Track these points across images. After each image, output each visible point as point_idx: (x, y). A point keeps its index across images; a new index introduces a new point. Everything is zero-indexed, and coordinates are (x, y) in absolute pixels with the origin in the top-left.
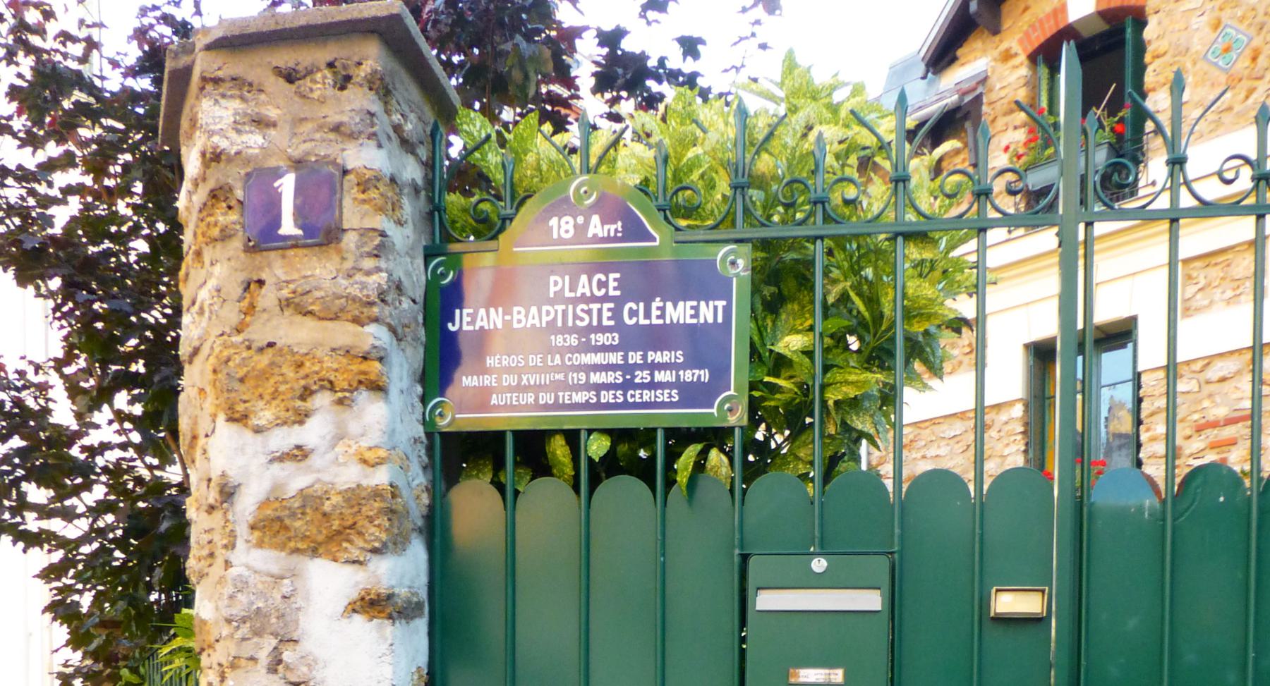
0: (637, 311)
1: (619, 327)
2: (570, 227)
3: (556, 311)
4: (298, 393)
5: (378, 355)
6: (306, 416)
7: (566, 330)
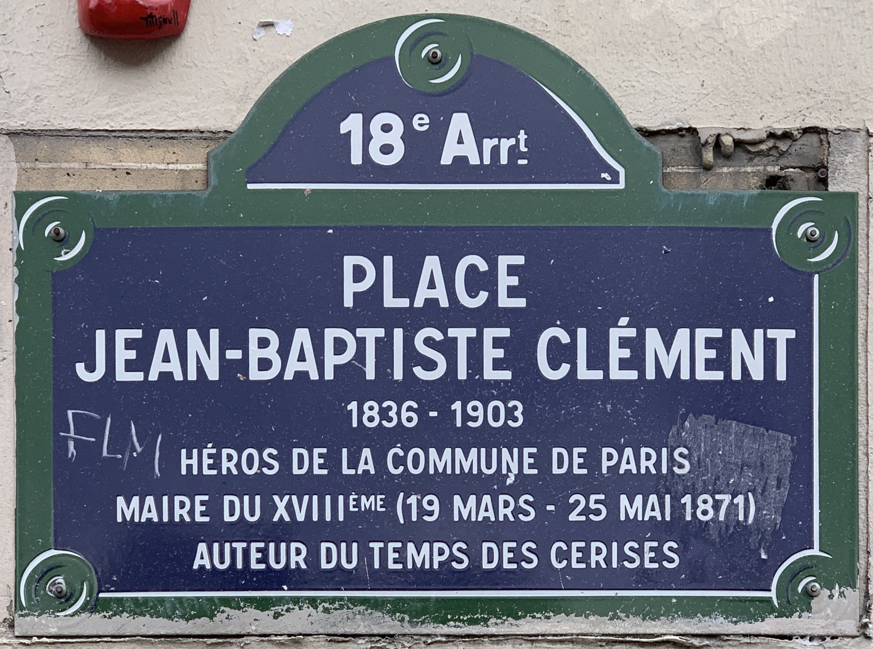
0: (573, 344)
2: (395, 138)
3: (361, 342)
7: (384, 388)
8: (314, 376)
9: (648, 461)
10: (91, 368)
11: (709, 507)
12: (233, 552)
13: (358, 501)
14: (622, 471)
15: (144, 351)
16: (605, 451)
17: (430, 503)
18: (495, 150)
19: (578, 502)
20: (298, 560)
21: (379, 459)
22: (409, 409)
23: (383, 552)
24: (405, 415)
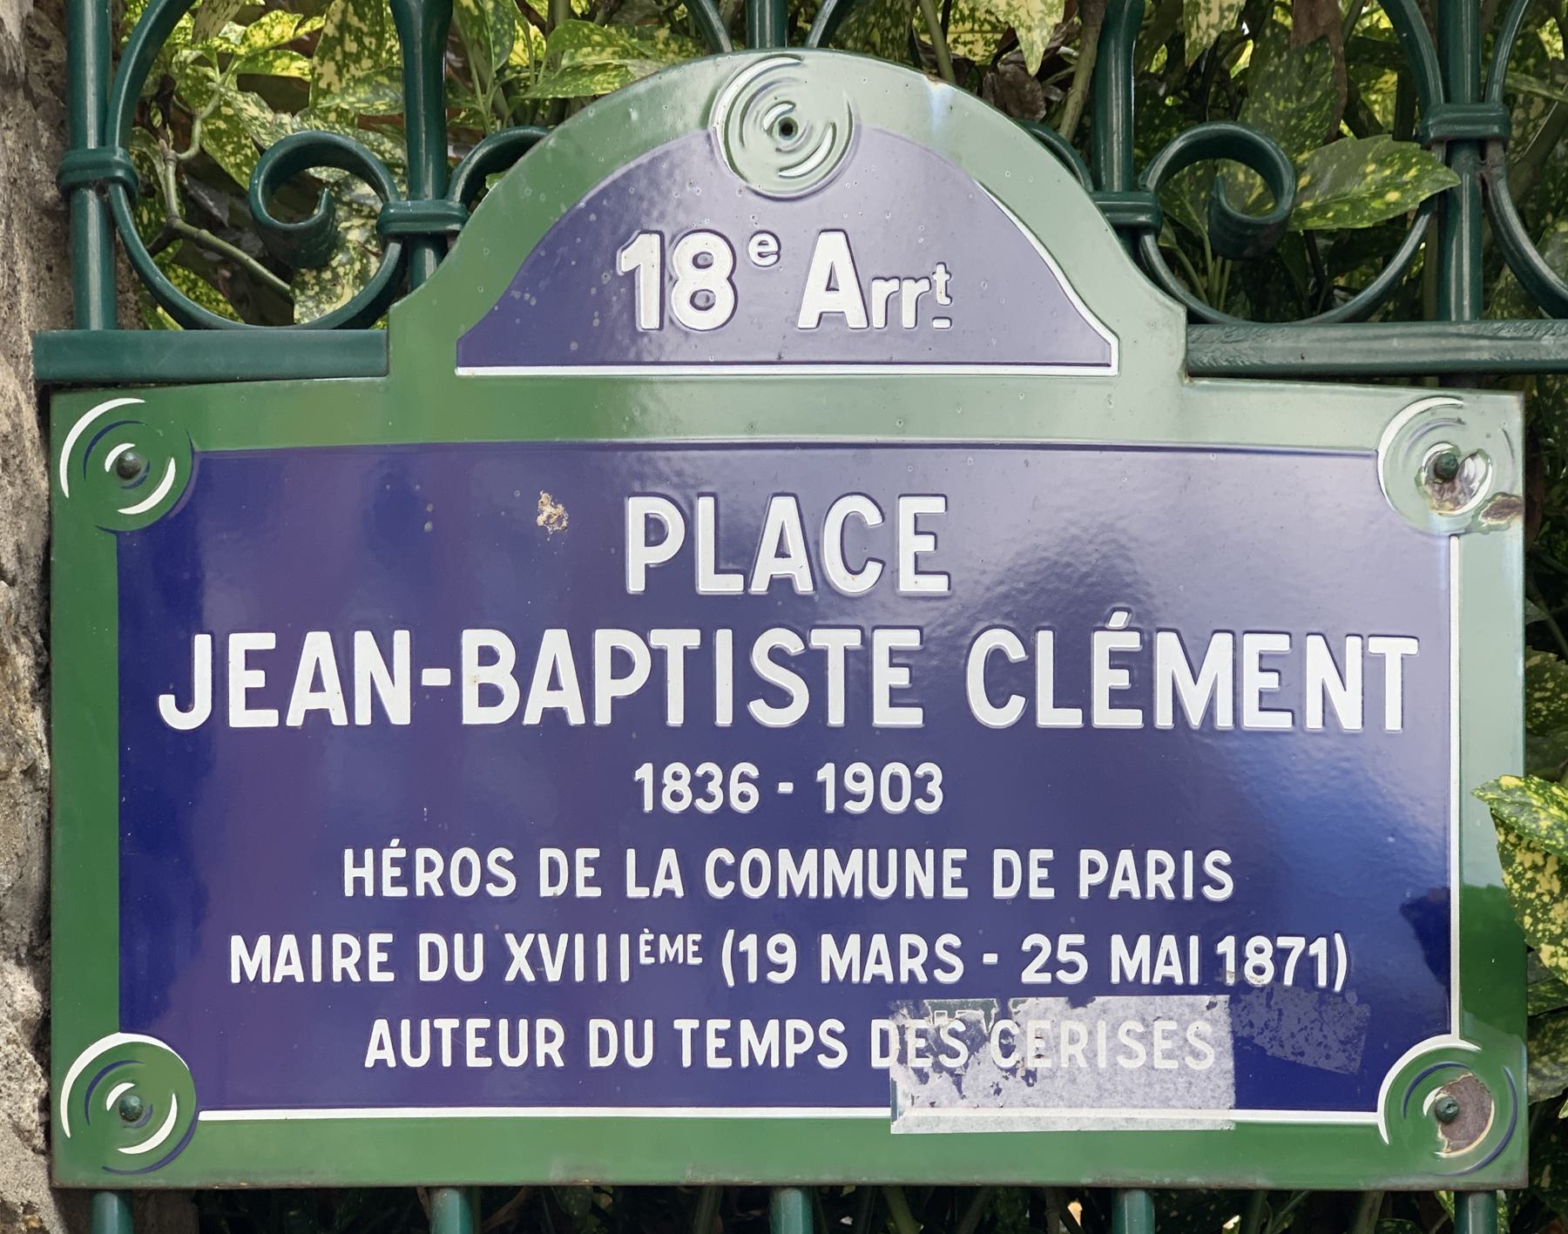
0: (1030, 665)
1: (946, 732)
2: (715, 280)
3: (659, 656)
7: (701, 741)
8: (576, 717)
9: (1156, 874)
10: (184, 704)
11: (1265, 960)
12: (436, 1035)
13: (654, 945)
14: (1114, 894)
15: (279, 670)
16: (1086, 855)
17: (781, 949)
19: (1037, 950)
20: (550, 1051)
21: (691, 872)
22: (744, 778)
23: (699, 1037)
24: (736, 788)
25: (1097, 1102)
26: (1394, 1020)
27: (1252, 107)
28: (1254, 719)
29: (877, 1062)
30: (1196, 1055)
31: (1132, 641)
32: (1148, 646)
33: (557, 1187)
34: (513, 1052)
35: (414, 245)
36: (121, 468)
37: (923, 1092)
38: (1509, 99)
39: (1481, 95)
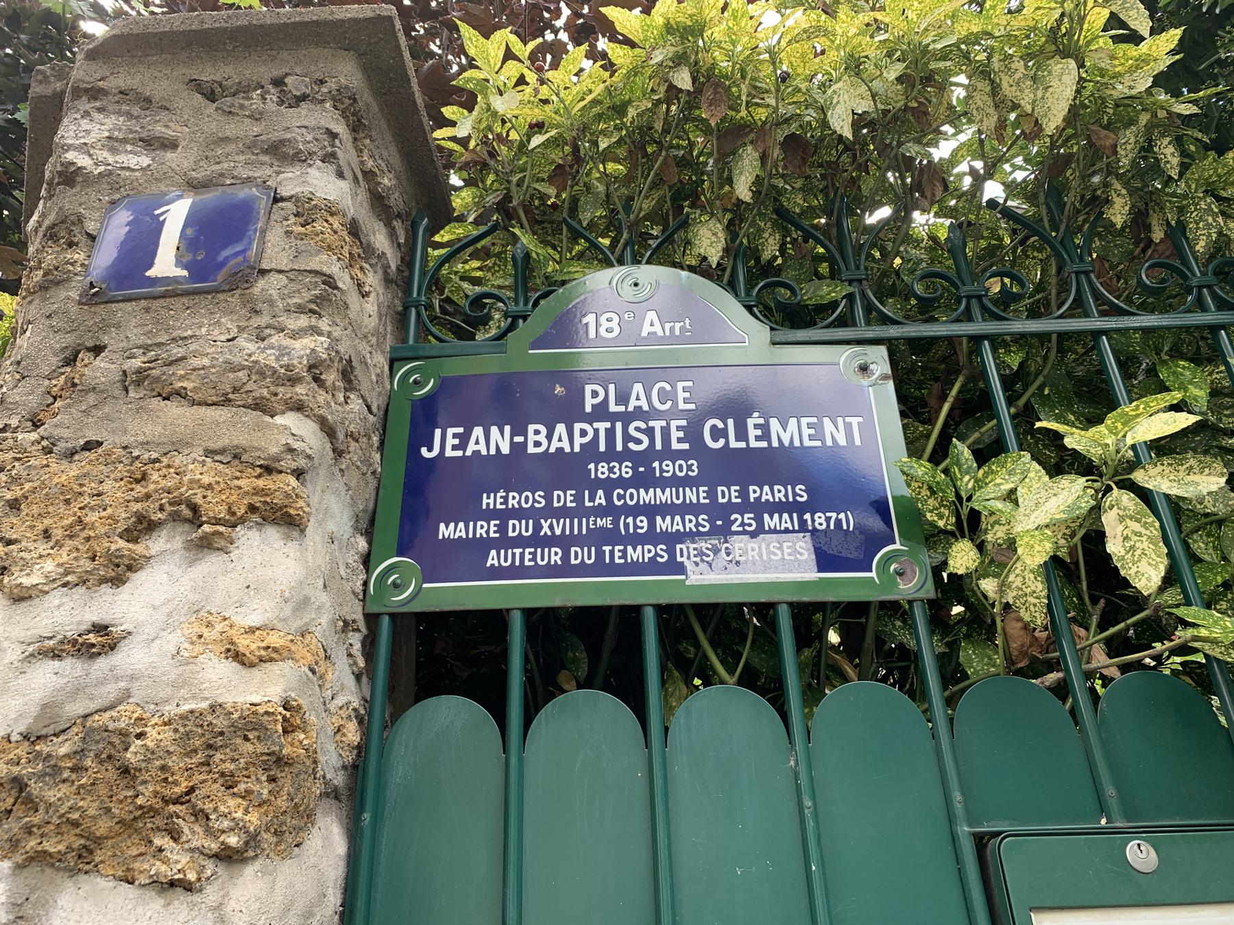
1: (697, 449)
2: (614, 324)
3: (596, 431)
4: (121, 527)
5: (294, 465)
6: (130, 568)
7: (611, 455)
8: (567, 450)
9: (779, 493)
10: (430, 450)
11: (823, 520)
12: (514, 555)
15: (464, 439)
16: (751, 488)
18: (672, 329)
19: (736, 519)
21: (609, 497)
23: (612, 553)
24: (624, 470)
25: (764, 572)
26: (873, 542)
27: (784, 274)
28: (807, 443)
29: (679, 559)
30: (801, 554)
31: (761, 421)
32: (767, 423)
33: (559, 608)
34: (543, 559)
35: (515, 319)
36: (415, 382)
37: (697, 569)
38: (866, 269)
39: (858, 268)
